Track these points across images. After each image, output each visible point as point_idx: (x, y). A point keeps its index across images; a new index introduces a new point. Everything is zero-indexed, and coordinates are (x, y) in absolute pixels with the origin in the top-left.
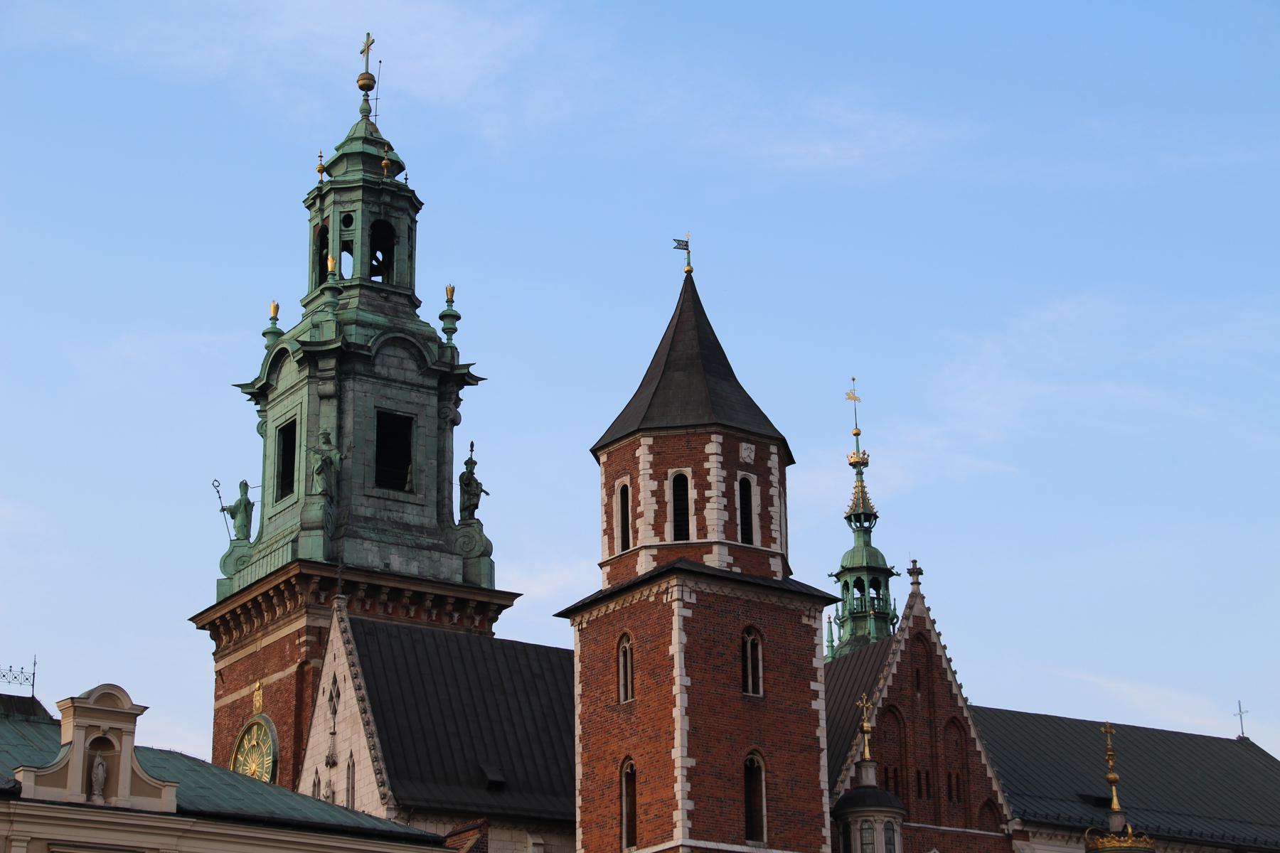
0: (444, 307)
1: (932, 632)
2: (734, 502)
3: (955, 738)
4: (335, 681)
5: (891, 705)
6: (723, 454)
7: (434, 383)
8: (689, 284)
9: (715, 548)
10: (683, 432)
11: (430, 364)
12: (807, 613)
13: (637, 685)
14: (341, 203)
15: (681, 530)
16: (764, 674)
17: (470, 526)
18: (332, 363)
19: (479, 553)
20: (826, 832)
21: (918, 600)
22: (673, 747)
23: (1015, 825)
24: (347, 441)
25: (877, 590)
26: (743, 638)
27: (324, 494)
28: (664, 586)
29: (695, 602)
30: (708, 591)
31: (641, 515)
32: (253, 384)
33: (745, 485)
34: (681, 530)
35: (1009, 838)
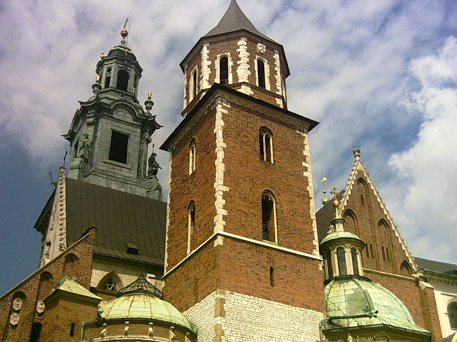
1: (368, 178)
3: (384, 230)
5: (349, 209)
6: (247, 46)
7: (140, 124)
9: (243, 87)
10: (225, 37)
11: (137, 115)
14: (107, 64)
16: (273, 153)
17: (152, 179)
18: (94, 111)
19: (155, 189)
22: (215, 182)
24: (97, 141)
26: (260, 134)
27: (82, 156)
28: (212, 102)
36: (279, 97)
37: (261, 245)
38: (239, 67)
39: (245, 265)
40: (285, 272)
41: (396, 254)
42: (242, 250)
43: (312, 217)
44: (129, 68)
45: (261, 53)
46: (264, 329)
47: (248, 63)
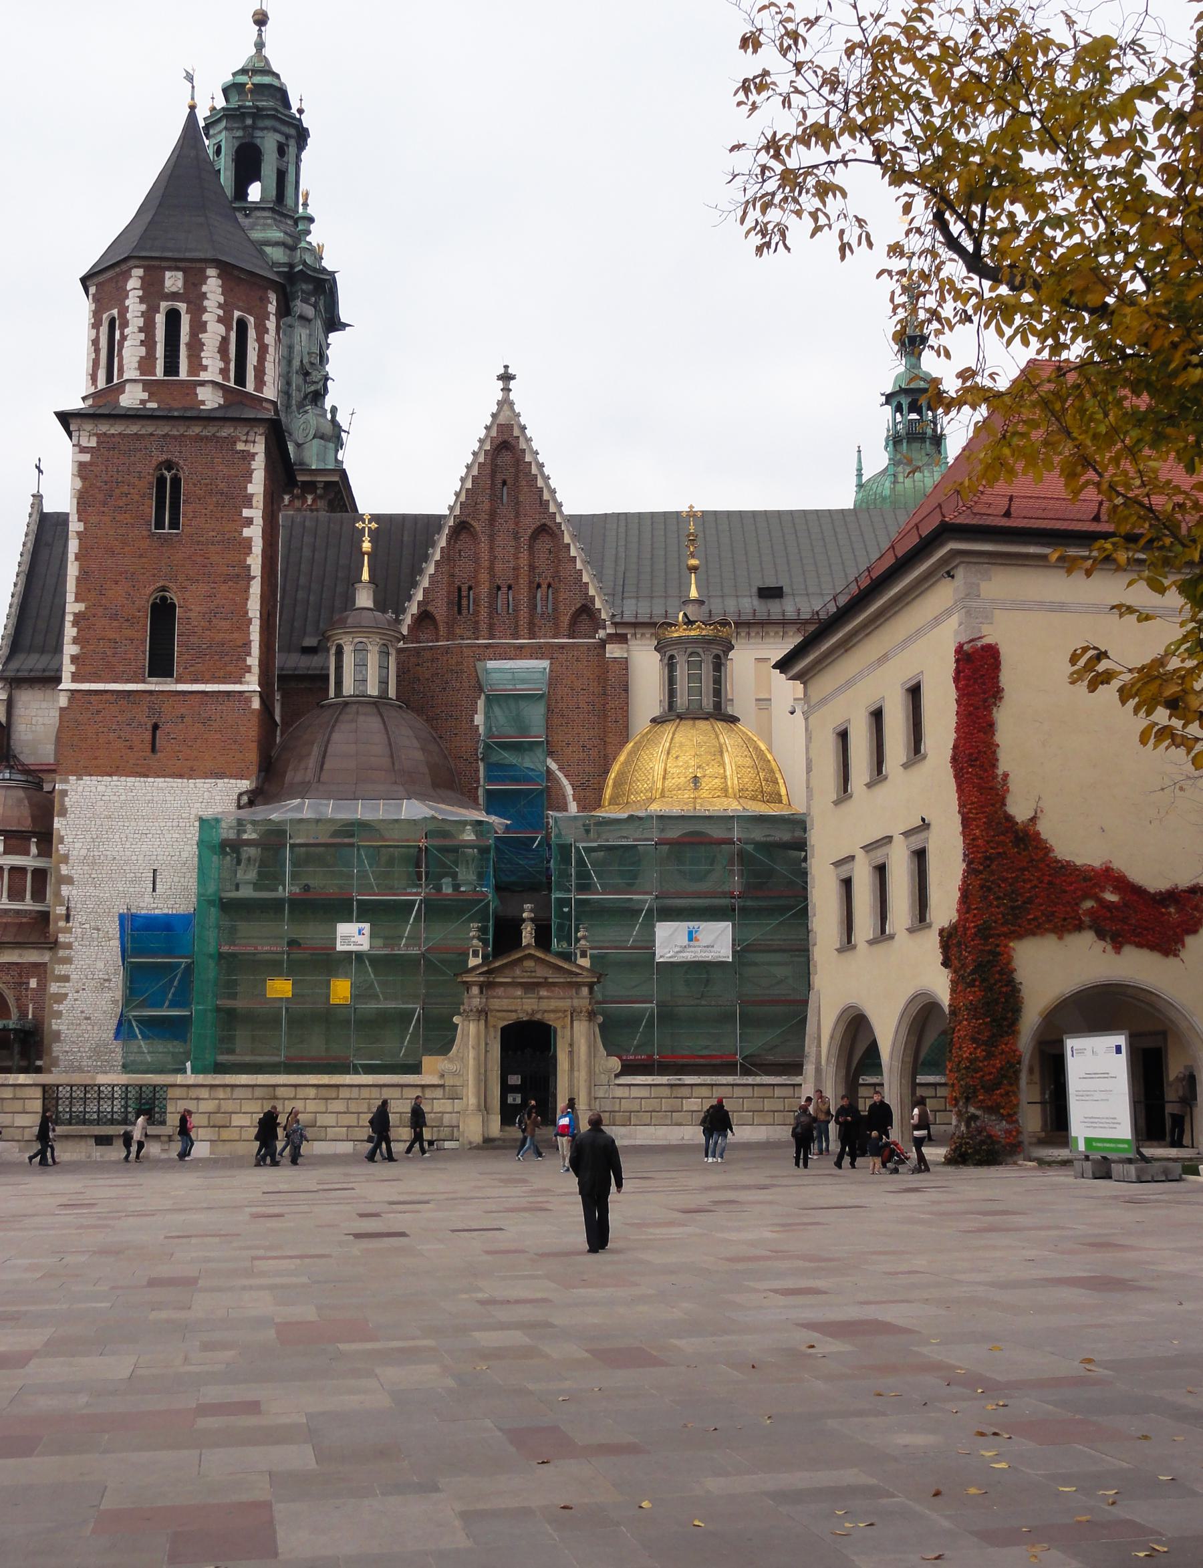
2: (154, 335)
3: (548, 547)
5: (463, 522)
6: (142, 288)
9: (128, 387)
12: (244, 438)
20: (253, 661)
21: (505, 407)
23: (609, 631)
25: (920, 413)
29: (95, 445)
30: (112, 431)
34: (109, 378)
35: (603, 644)
36: (203, 383)
37: (137, 691)
38: (126, 343)
39: (106, 730)
40: (181, 726)
41: (562, 596)
42: (101, 706)
43: (251, 615)
44: (258, 133)
45: (174, 293)
46: (135, 824)
47: (141, 330)
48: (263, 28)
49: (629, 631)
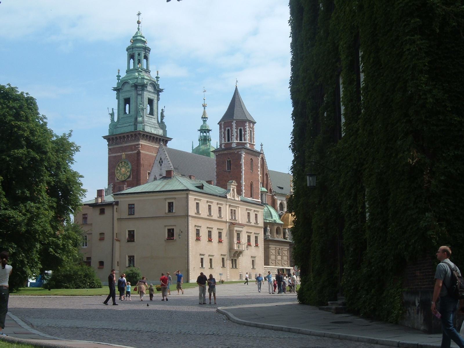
0: (157, 76)
4: (161, 159)
7: (156, 92)
8: (236, 88)
9: (247, 143)
13: (232, 167)
14: (138, 51)
15: (241, 140)
18: (140, 87)
20: (260, 196)
21: (262, 151)
23: (274, 193)
31: (233, 136)
32: (116, 88)
33: (251, 131)
34: (241, 140)
48: (140, 25)
49: (276, 194)
